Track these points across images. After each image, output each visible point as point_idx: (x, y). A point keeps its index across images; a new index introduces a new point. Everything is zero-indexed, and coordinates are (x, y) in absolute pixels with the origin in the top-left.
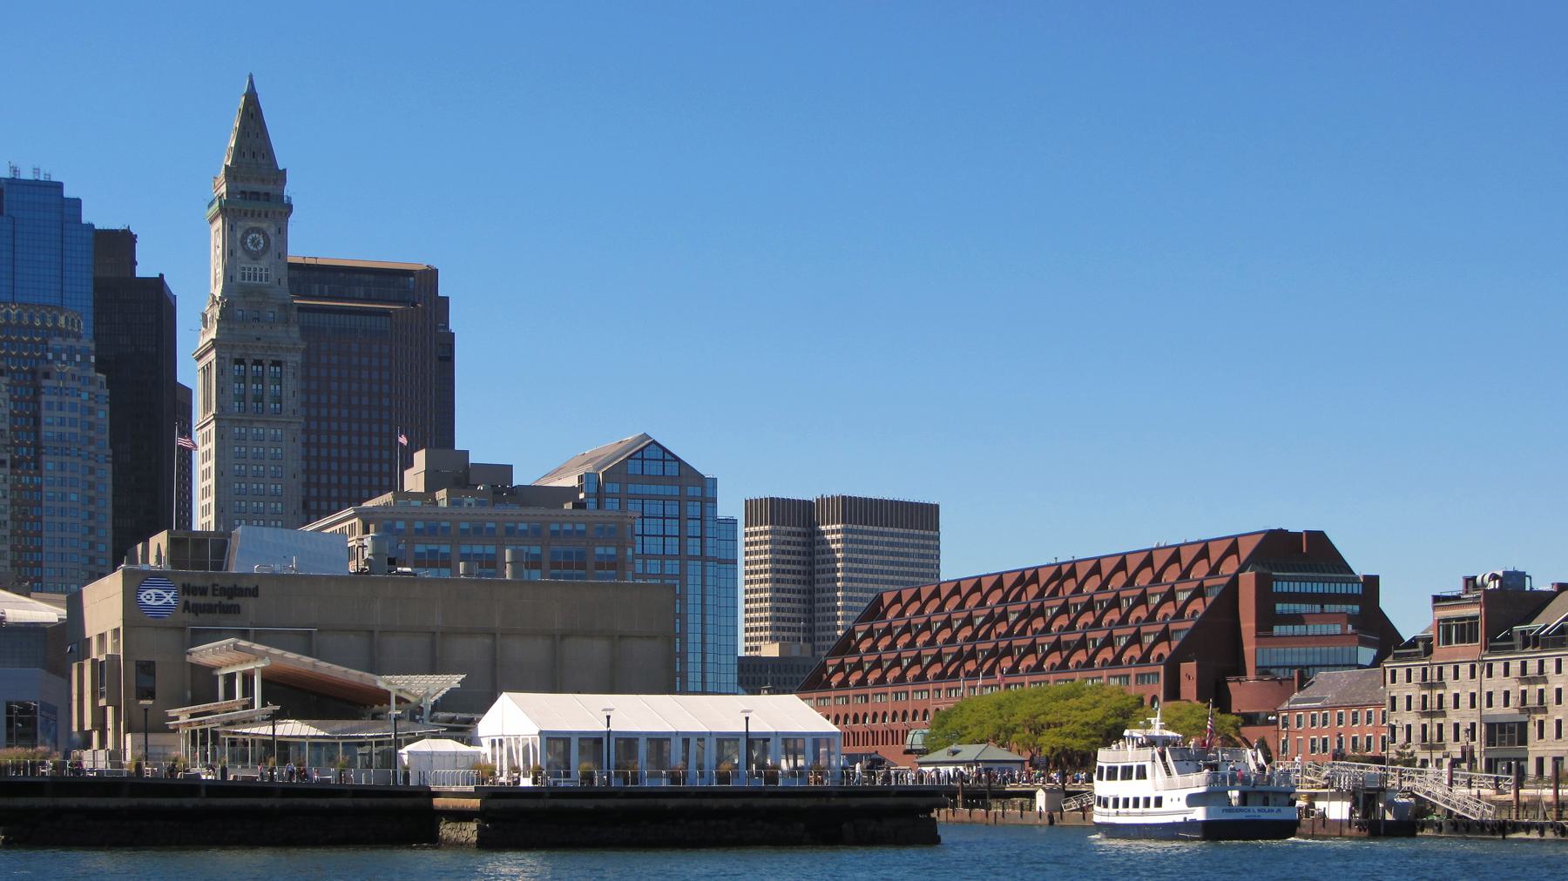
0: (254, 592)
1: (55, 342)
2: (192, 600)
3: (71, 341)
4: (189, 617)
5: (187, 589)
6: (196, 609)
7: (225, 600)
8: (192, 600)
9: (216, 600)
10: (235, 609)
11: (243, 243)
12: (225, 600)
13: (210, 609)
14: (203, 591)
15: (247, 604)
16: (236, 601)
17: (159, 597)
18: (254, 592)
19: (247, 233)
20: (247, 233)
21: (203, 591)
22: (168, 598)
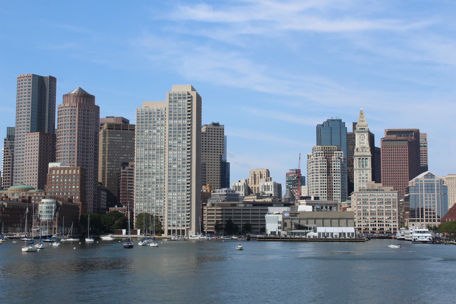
0: (299, 214)
1: (336, 152)
2: (291, 215)
3: (339, 152)
4: (291, 217)
5: (291, 214)
6: (292, 216)
7: (295, 215)
8: (291, 215)
9: (294, 215)
10: (296, 216)
11: (360, 137)
12: (295, 215)
13: (293, 216)
14: (292, 214)
15: (298, 215)
16: (297, 215)
17: (287, 215)
18: (299, 214)
19: (361, 136)
20: (361, 136)
21: (292, 214)
22: (288, 215)
